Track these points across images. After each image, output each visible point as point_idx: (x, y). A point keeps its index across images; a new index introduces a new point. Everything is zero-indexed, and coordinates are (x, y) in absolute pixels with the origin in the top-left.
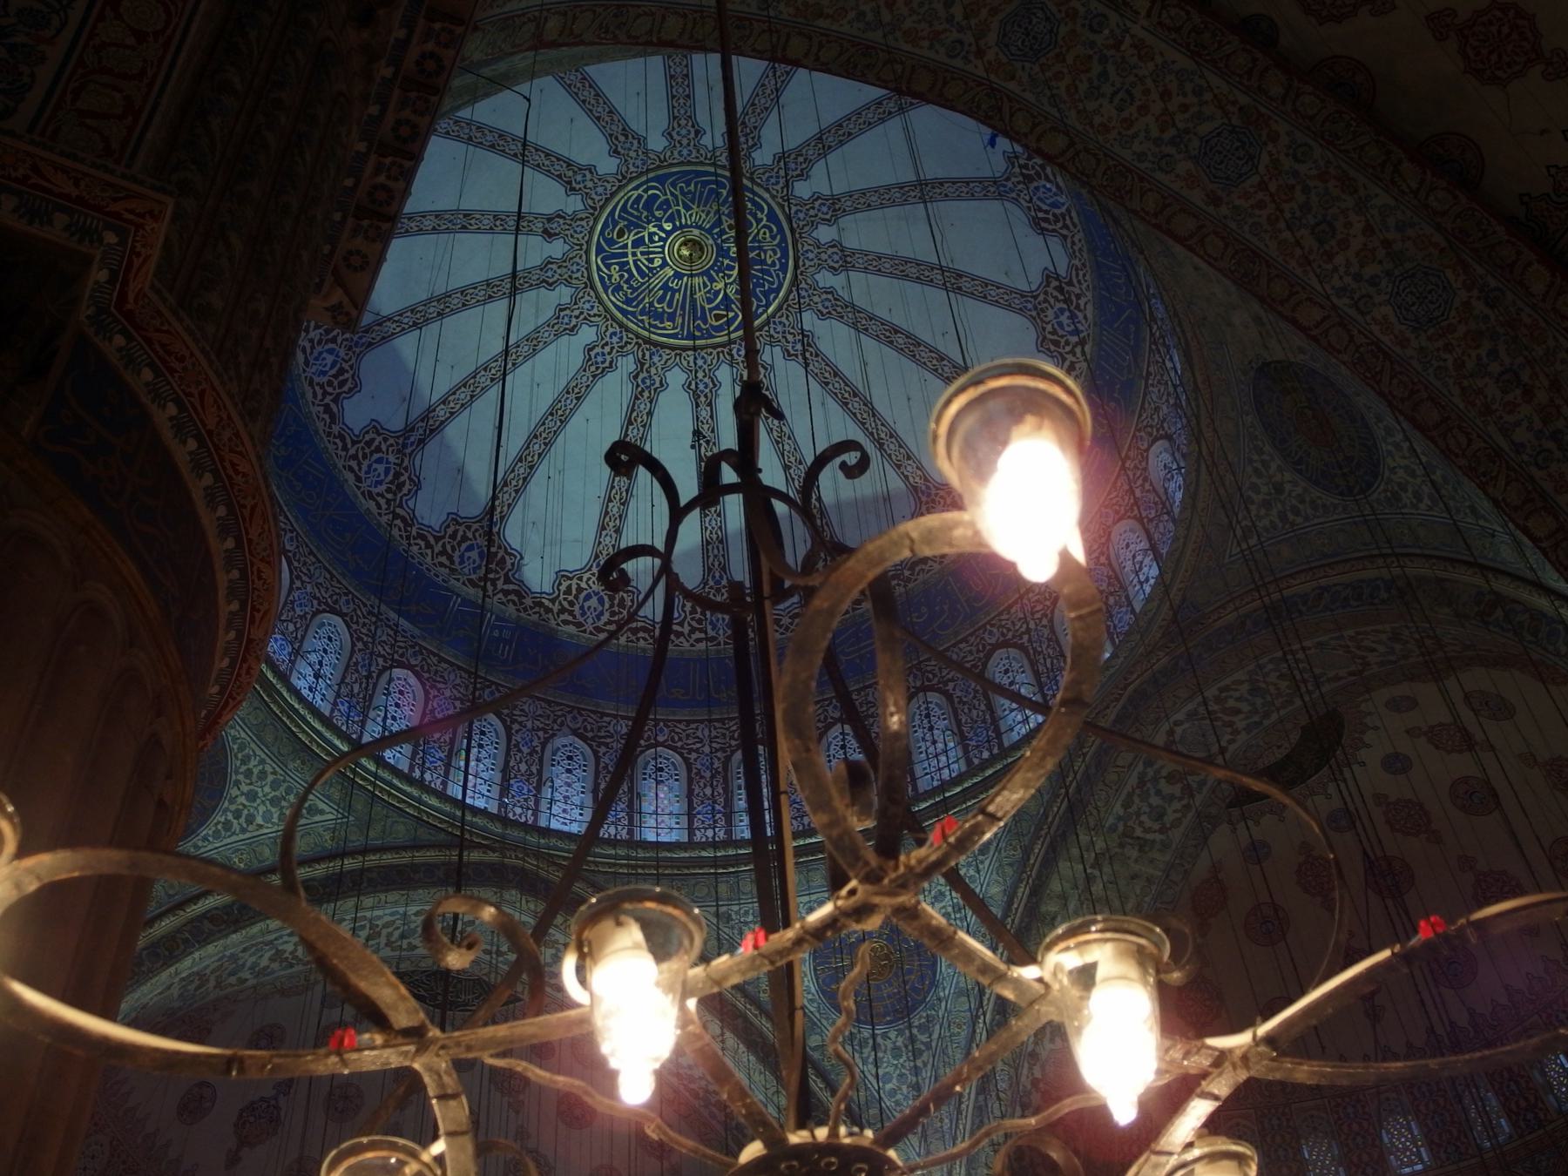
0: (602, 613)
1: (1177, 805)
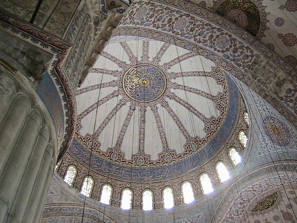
0: (214, 126)
1: (245, 51)
